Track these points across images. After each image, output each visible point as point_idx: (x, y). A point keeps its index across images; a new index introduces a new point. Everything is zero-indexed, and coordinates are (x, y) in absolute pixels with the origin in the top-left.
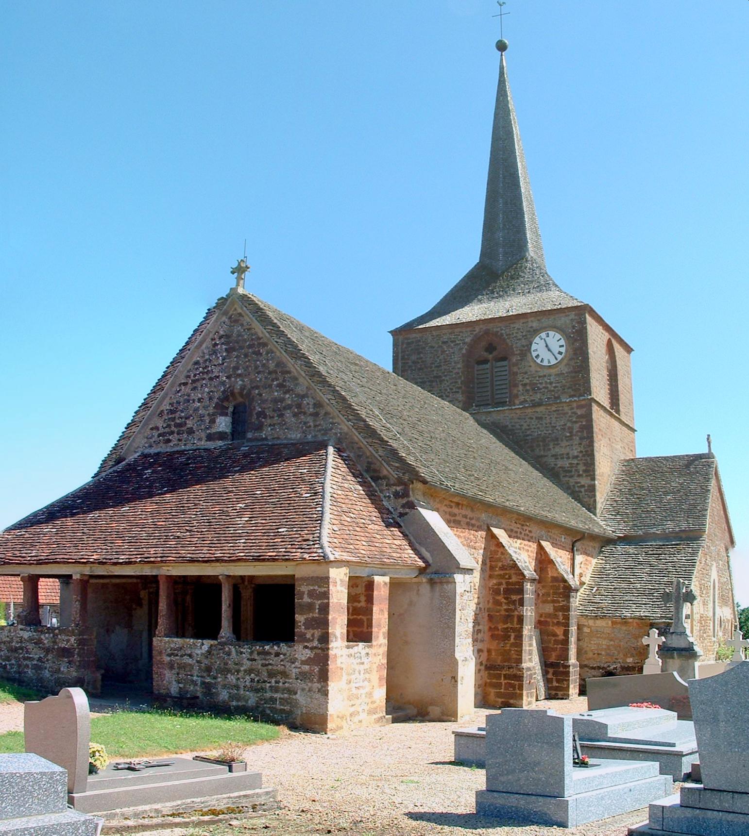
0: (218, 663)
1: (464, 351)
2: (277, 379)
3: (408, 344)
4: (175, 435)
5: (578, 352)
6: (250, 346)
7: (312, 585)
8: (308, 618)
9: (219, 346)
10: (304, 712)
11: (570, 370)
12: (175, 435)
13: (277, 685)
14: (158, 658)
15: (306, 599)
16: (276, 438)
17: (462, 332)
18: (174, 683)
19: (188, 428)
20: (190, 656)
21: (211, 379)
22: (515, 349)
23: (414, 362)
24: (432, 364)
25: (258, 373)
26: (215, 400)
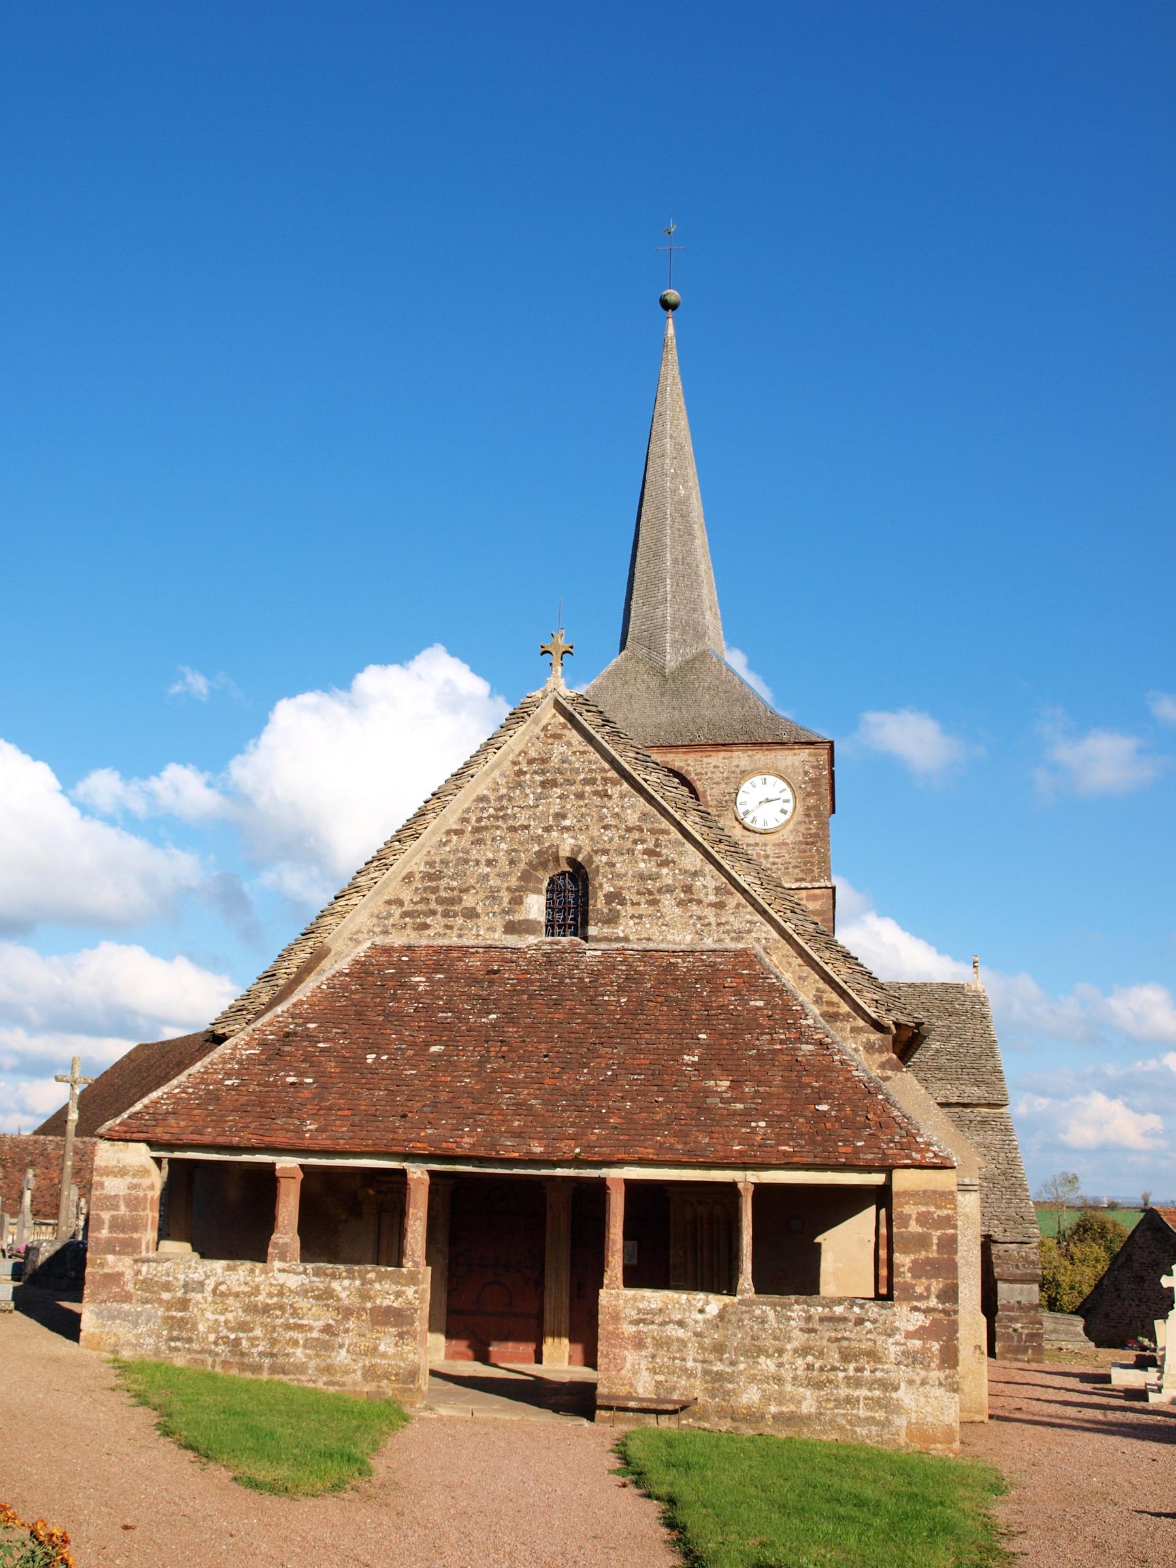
0: (740, 1336)
2: (643, 841)
4: (439, 916)
5: (812, 813)
6: (586, 782)
7: (927, 1204)
8: (918, 1259)
9: (528, 776)
10: (914, 1421)
11: (798, 840)
12: (439, 916)
13: (859, 1374)
14: (610, 1328)
15: (914, 1227)
16: (645, 938)
18: (645, 1374)
19: (465, 908)
20: (681, 1324)
21: (513, 829)
22: (709, 798)
25: (606, 827)
26: (522, 866)
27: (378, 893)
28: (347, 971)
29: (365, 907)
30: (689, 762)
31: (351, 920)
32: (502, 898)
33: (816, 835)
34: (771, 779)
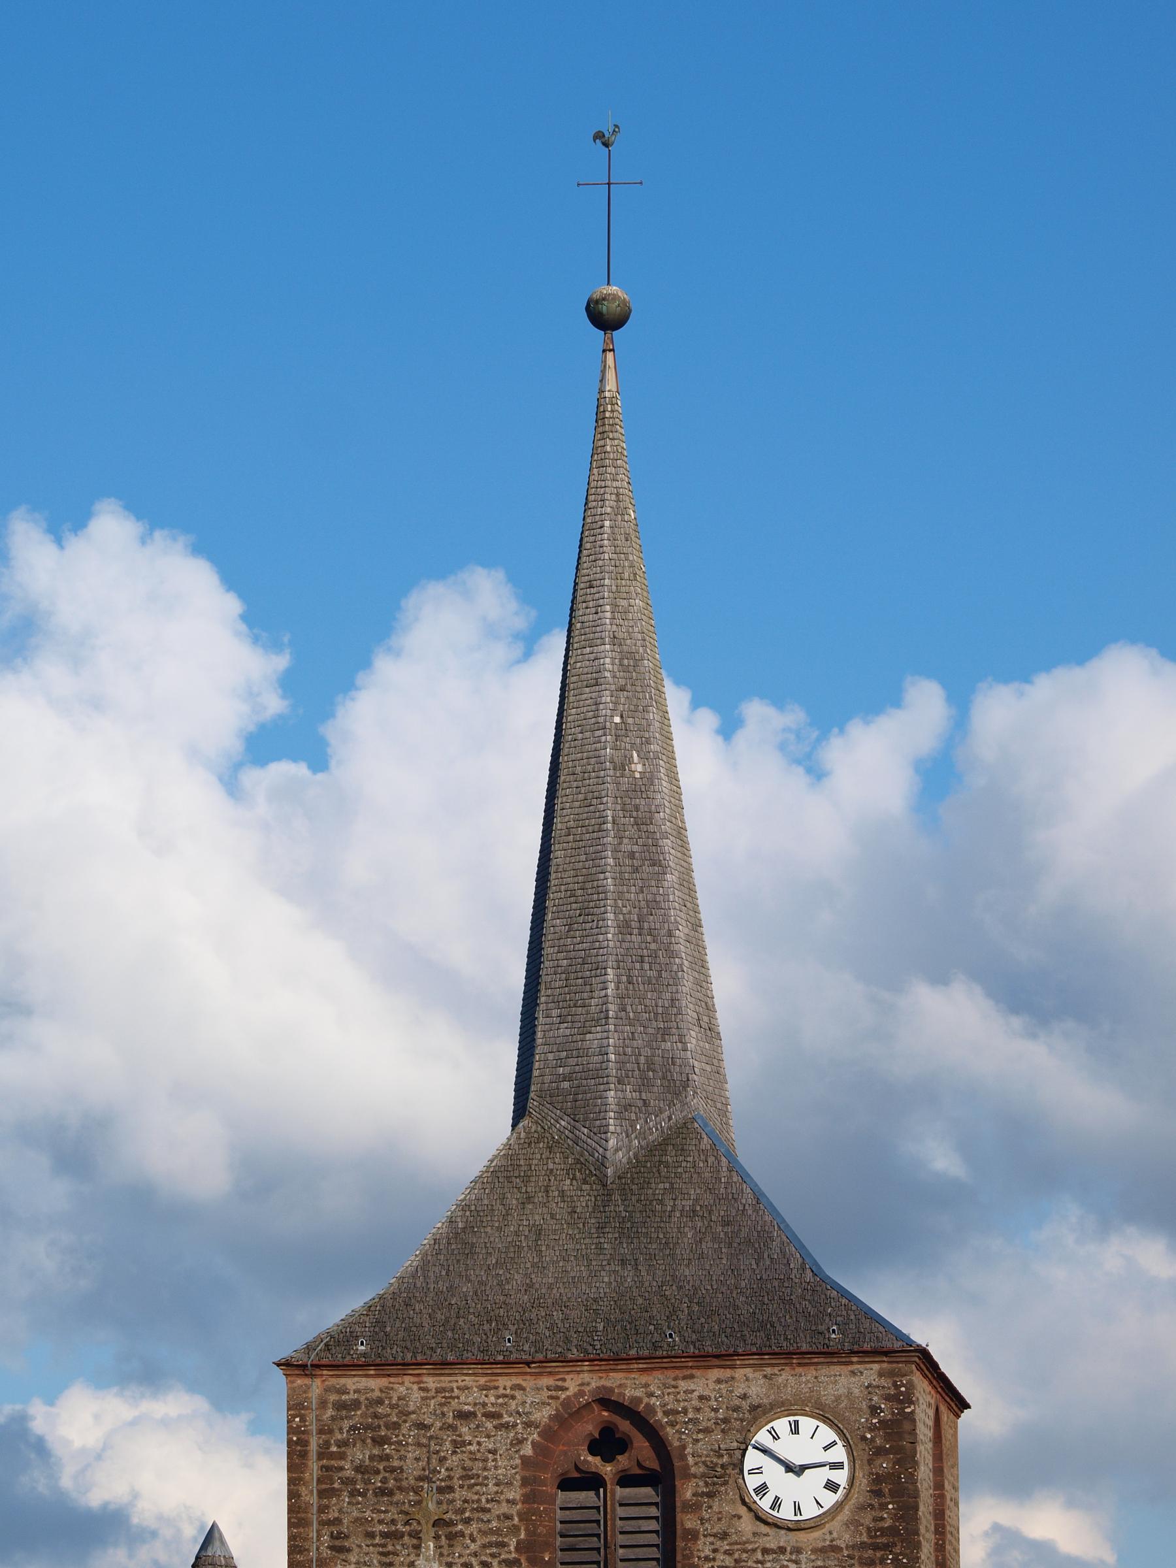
1: (528, 1450)
3: (340, 1406)
17: (524, 1389)
22: (690, 1460)
23: (357, 1469)
24: (420, 1479)
30: (652, 1388)
33: (892, 1531)
34: (807, 1424)
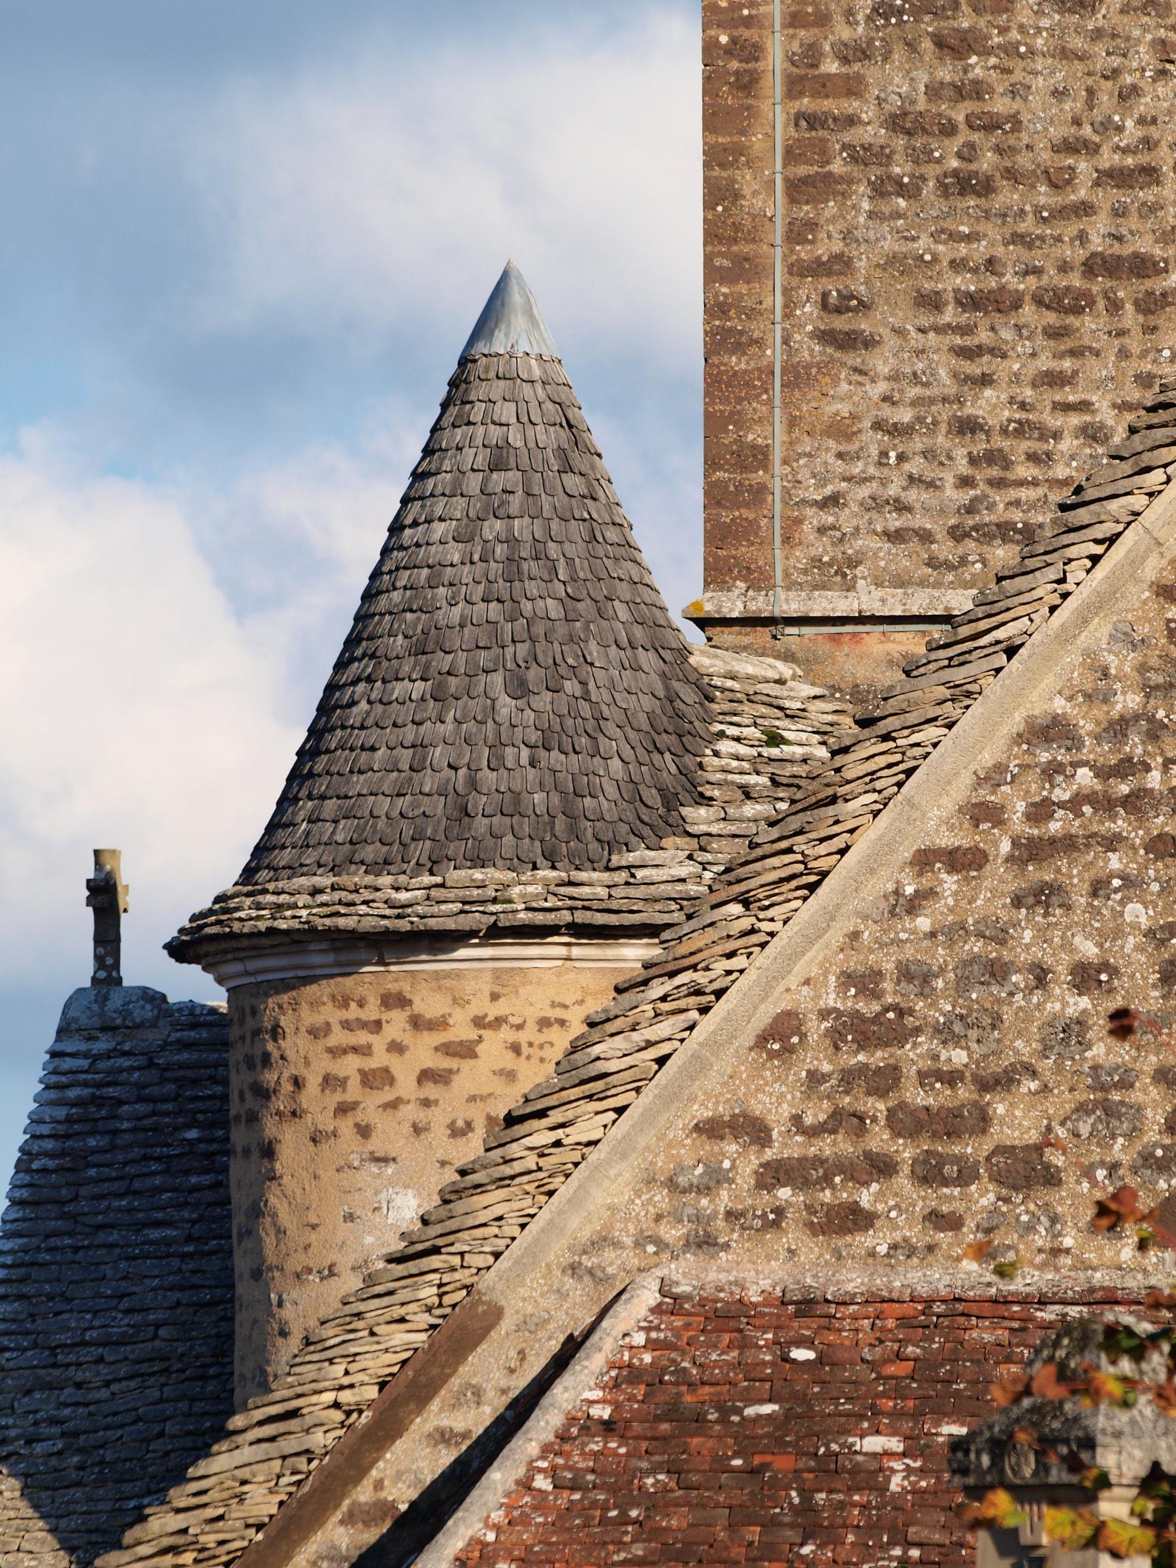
4: (903, 1181)
12: (903, 1181)
19: (999, 1150)
23: (896, 122)
27: (670, 1098)
28: (603, 1412)
29: (622, 1152)
31: (574, 1202)
32: (1139, 1109)
